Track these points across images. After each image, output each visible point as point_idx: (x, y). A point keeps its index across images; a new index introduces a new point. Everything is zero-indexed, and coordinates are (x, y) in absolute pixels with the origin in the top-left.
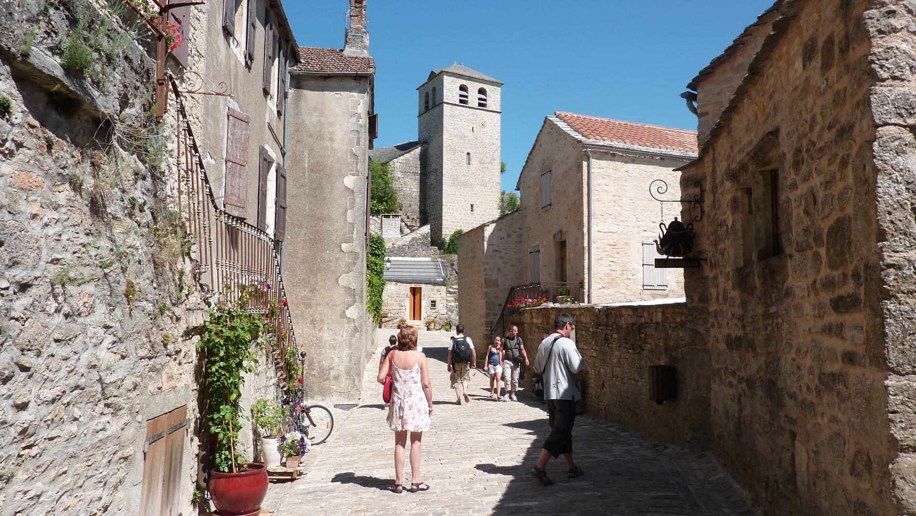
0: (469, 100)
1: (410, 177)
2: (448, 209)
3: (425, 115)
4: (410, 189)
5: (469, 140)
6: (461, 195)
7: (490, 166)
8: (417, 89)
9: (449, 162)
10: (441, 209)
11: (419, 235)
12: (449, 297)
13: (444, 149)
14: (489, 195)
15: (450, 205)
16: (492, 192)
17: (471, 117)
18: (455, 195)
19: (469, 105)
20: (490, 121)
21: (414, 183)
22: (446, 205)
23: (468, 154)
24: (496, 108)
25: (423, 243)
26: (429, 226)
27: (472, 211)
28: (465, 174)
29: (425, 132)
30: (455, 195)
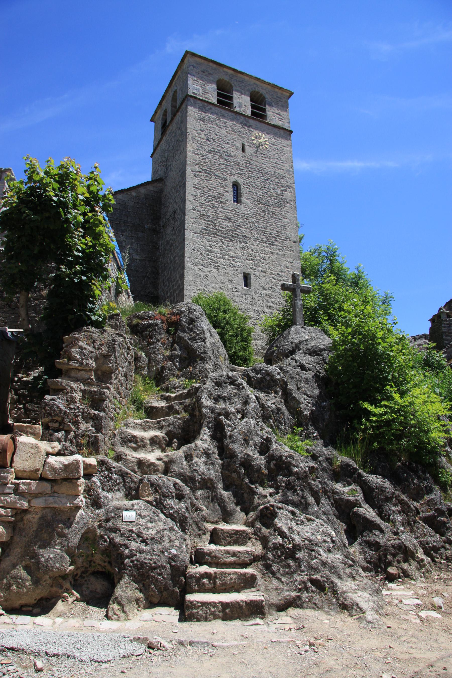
7: (277, 211)
8: (152, 120)
10: (182, 276)
12: (145, 428)
13: (189, 169)
23: (236, 186)
28: (230, 216)
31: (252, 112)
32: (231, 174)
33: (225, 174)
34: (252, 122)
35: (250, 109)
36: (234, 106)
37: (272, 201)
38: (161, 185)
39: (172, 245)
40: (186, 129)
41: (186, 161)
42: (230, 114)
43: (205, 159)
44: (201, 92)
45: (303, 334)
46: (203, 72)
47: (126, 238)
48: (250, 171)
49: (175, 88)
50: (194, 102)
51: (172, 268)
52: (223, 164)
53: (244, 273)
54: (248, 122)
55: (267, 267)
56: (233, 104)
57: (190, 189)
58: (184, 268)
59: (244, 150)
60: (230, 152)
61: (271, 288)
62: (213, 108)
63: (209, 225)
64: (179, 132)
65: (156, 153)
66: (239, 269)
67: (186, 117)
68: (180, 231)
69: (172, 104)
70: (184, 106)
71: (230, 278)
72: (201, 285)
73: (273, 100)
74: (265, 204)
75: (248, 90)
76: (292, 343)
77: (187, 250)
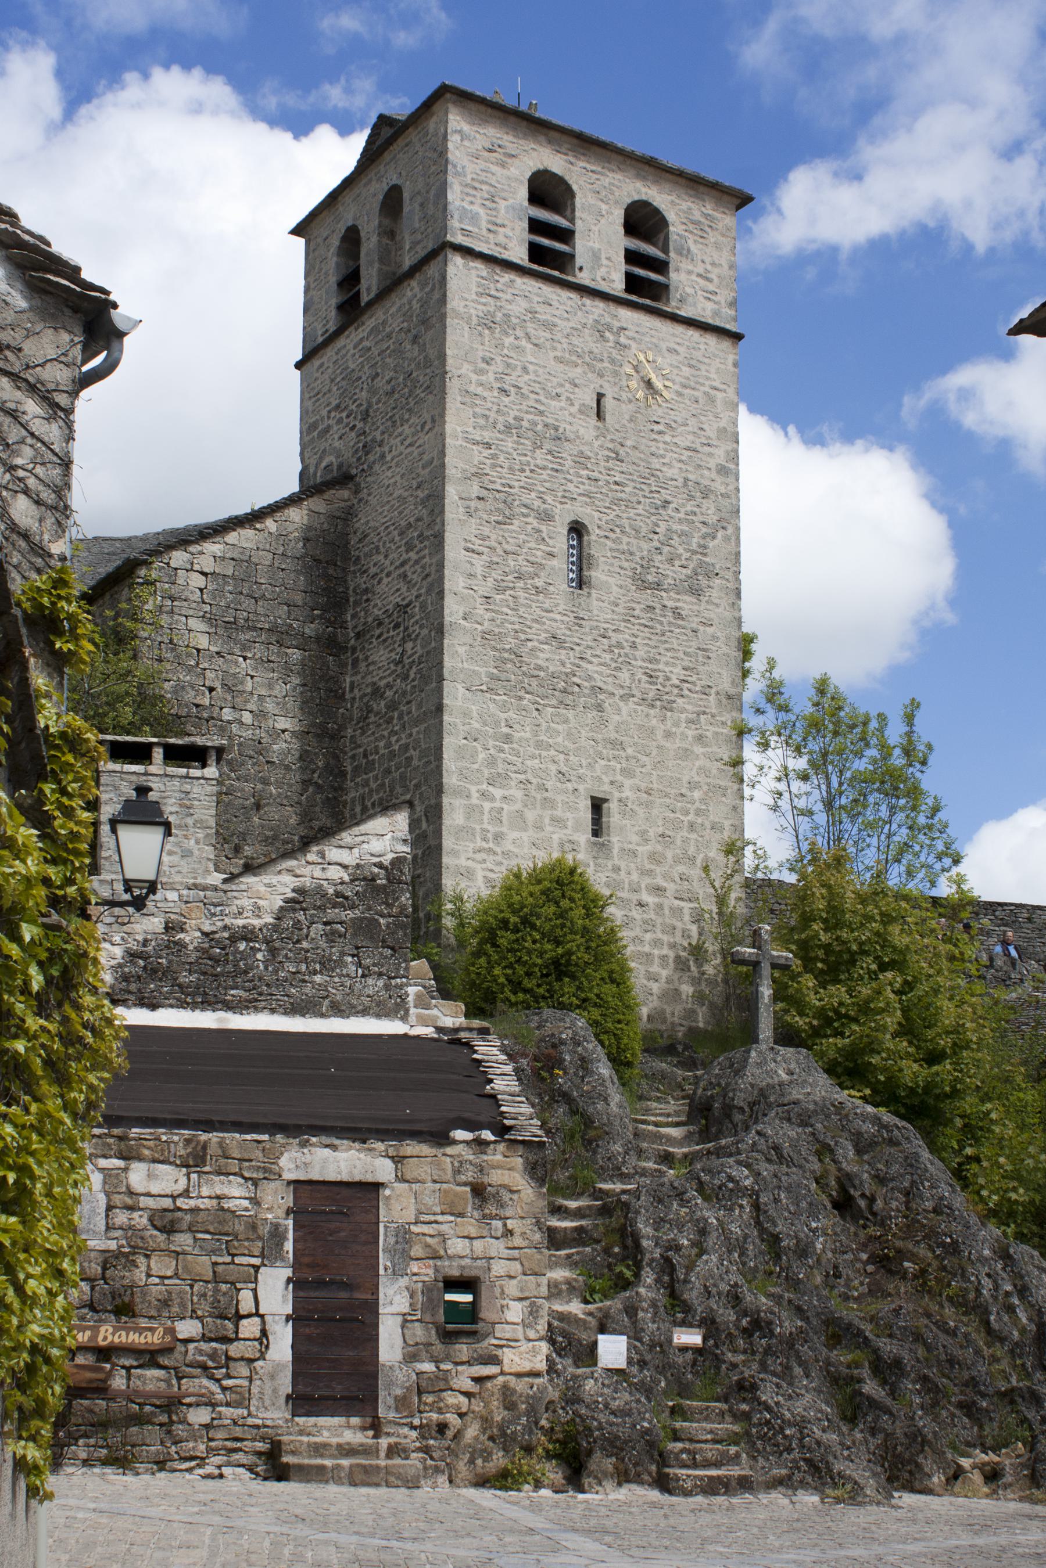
0: (582, 248)
1: (258, 650)
2: (471, 811)
3: (341, 342)
4: (260, 715)
5: (581, 460)
7: (686, 603)
8: (298, 231)
11: (336, 873)
13: (451, 492)
14: (686, 754)
16: (700, 738)
17: (587, 342)
18: (508, 739)
19: (583, 278)
20: (686, 371)
21: (280, 689)
22: (458, 792)
23: (577, 529)
24: (716, 313)
25: (365, 928)
26: (401, 821)
27: (596, 833)
28: (561, 631)
29: (336, 430)
31: (630, 278)
32: (568, 498)
33: (549, 499)
34: (626, 315)
36: (577, 265)
37: (673, 573)
38: (345, 493)
39: (392, 706)
40: (442, 357)
41: (443, 465)
42: (565, 294)
44: (484, 225)
45: (773, 1065)
46: (490, 151)
47: (256, 669)
48: (616, 483)
50: (465, 265)
51: (397, 775)
52: (544, 468)
53: (593, 798)
55: (654, 778)
56: (572, 257)
57: (454, 551)
58: (439, 790)
59: (600, 415)
60: (563, 425)
61: (662, 835)
63: (504, 661)
64: (411, 351)
65: (316, 362)
66: (581, 788)
67: (443, 317)
68: (425, 679)
69: (380, 226)
70: (432, 270)
71: (559, 813)
72: (485, 839)
73: (691, 227)
74: (658, 586)
75: (617, 202)
76: (752, 1085)
77: (447, 741)
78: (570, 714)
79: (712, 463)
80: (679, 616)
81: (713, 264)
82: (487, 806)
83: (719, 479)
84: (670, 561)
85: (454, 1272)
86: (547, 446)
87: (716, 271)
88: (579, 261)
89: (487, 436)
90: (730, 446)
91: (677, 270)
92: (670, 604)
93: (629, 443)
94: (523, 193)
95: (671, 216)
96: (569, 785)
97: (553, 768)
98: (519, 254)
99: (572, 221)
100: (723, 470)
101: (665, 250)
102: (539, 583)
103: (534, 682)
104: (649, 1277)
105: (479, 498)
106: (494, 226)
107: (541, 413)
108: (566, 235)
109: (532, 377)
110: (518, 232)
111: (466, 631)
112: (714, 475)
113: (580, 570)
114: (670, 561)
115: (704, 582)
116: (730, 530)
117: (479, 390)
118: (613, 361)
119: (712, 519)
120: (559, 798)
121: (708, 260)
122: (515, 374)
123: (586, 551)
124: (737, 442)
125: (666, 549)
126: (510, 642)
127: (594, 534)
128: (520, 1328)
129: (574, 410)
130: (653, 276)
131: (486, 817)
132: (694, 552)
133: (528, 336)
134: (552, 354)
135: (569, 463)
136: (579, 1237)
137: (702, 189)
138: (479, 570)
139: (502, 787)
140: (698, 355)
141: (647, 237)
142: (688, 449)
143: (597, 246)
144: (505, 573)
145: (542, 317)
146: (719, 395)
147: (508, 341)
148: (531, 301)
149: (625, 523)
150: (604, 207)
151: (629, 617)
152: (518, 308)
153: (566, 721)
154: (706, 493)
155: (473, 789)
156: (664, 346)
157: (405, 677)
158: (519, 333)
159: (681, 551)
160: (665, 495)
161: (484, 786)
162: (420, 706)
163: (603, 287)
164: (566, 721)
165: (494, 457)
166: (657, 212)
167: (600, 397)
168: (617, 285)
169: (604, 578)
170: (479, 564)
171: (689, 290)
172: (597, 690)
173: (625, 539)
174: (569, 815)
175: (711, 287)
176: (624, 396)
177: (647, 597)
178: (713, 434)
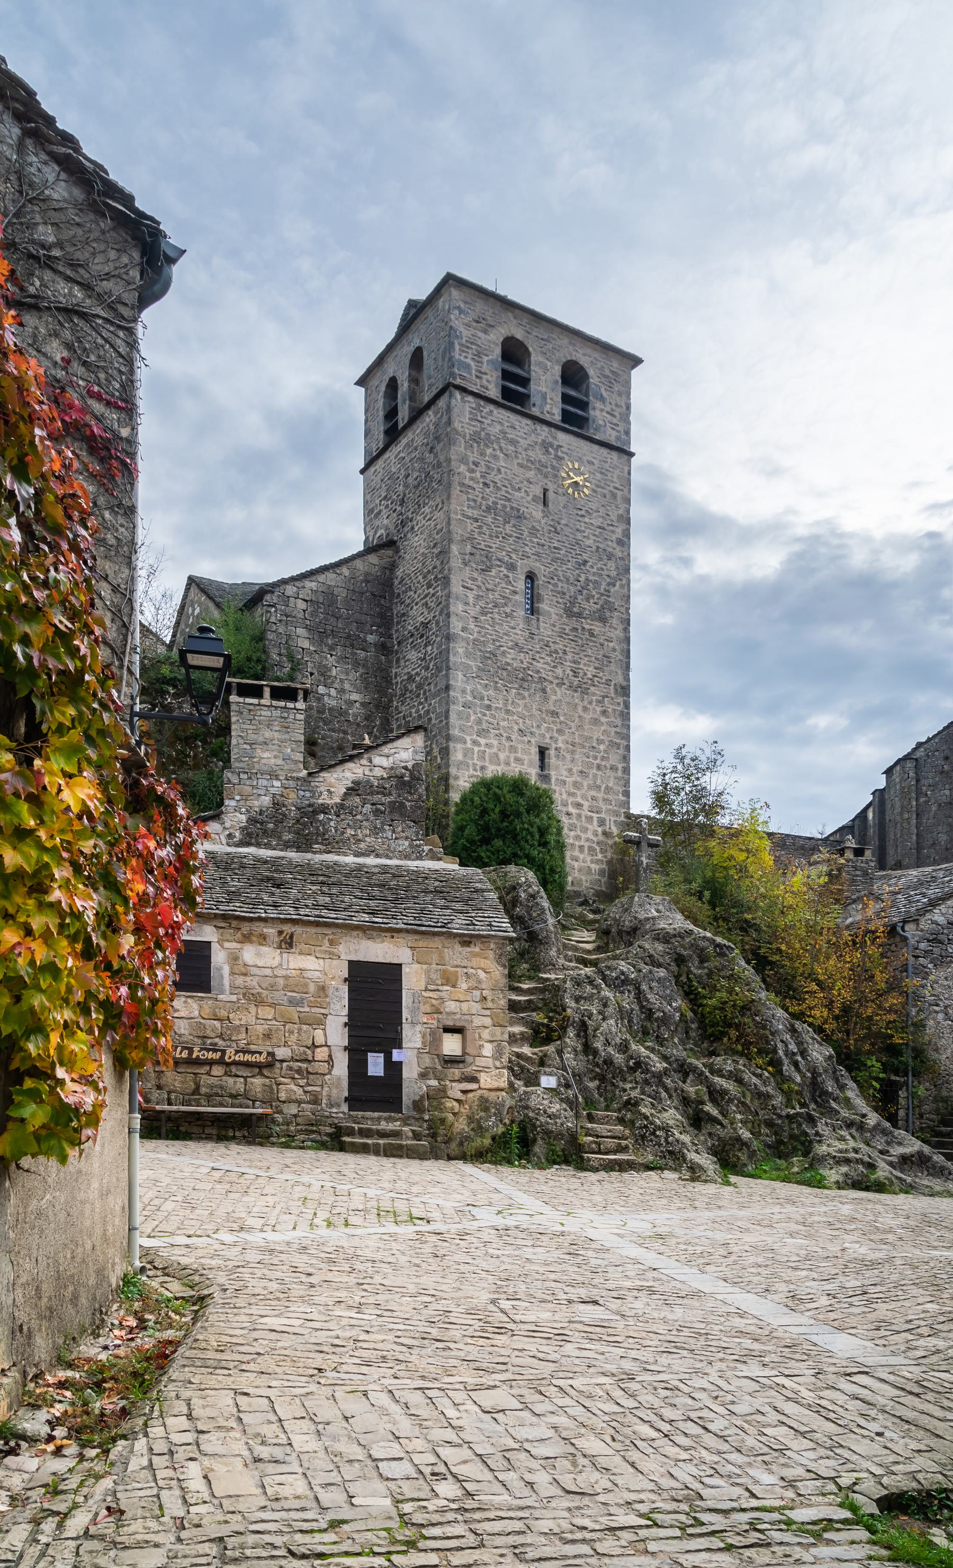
2: (467, 752)
5: (534, 531)
6: (508, 712)
7: (597, 627)
9: (469, 593)
13: (455, 548)
15: (475, 742)
17: (537, 454)
18: (489, 707)
19: (535, 411)
20: (599, 476)
28: (521, 641)
30: (489, 707)
31: (565, 413)
32: (525, 556)
33: (514, 556)
34: (563, 437)
35: (560, 405)
37: (590, 607)
43: (480, 527)
49: (417, 343)
52: (511, 536)
54: (555, 438)
56: (528, 396)
59: (545, 503)
60: (522, 509)
62: (495, 411)
66: (533, 740)
71: (519, 755)
72: (475, 770)
78: (526, 694)
79: (614, 538)
80: (592, 635)
81: (617, 405)
82: (476, 749)
83: (618, 548)
84: (588, 600)
85: (450, 1023)
86: (513, 522)
87: (618, 410)
88: (533, 400)
89: (475, 513)
90: (624, 526)
91: (594, 409)
92: (587, 627)
93: (563, 522)
94: (498, 351)
95: (591, 372)
96: (526, 739)
97: (516, 728)
98: (494, 392)
99: (529, 372)
100: (620, 542)
101: (587, 395)
102: (508, 610)
103: (505, 673)
104: (571, 1033)
105: (471, 554)
106: (480, 374)
107: (509, 500)
108: (525, 382)
109: (503, 475)
110: (494, 378)
111: (463, 639)
112: (615, 545)
113: (532, 603)
114: (588, 600)
115: (608, 614)
116: (624, 582)
117: (471, 483)
118: (553, 467)
119: (613, 573)
120: (520, 746)
121: (613, 402)
122: (493, 473)
123: (535, 592)
124: (629, 524)
125: (585, 592)
126: (490, 647)
127: (541, 580)
128: (490, 1060)
129: (529, 498)
130: (580, 412)
131: (476, 756)
132: (602, 595)
133: (501, 449)
134: (516, 461)
135: (526, 533)
136: (529, 1006)
137: (610, 353)
138: (471, 600)
139: (485, 737)
140: (607, 466)
141: (576, 387)
142: (599, 527)
143: (544, 390)
144: (487, 603)
145: (510, 436)
146: (619, 493)
147: (489, 451)
148: (502, 425)
149: (560, 573)
150: (549, 364)
151: (562, 634)
152: (495, 430)
153: (524, 698)
154: (610, 557)
155: (468, 738)
156: (585, 459)
157: (427, 668)
158: (495, 446)
159: (594, 593)
160: (585, 557)
161: (475, 737)
162: (436, 685)
163: (547, 417)
164: (524, 698)
165: (480, 527)
166: (582, 368)
167: (545, 491)
168: (557, 417)
169: (547, 608)
170: (471, 596)
171: (601, 422)
172: (542, 680)
173: (560, 584)
174: (525, 757)
175: (615, 421)
176: (560, 490)
177: (573, 623)
178: (615, 519)
